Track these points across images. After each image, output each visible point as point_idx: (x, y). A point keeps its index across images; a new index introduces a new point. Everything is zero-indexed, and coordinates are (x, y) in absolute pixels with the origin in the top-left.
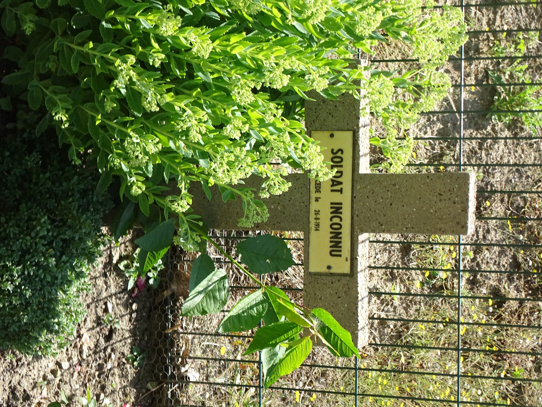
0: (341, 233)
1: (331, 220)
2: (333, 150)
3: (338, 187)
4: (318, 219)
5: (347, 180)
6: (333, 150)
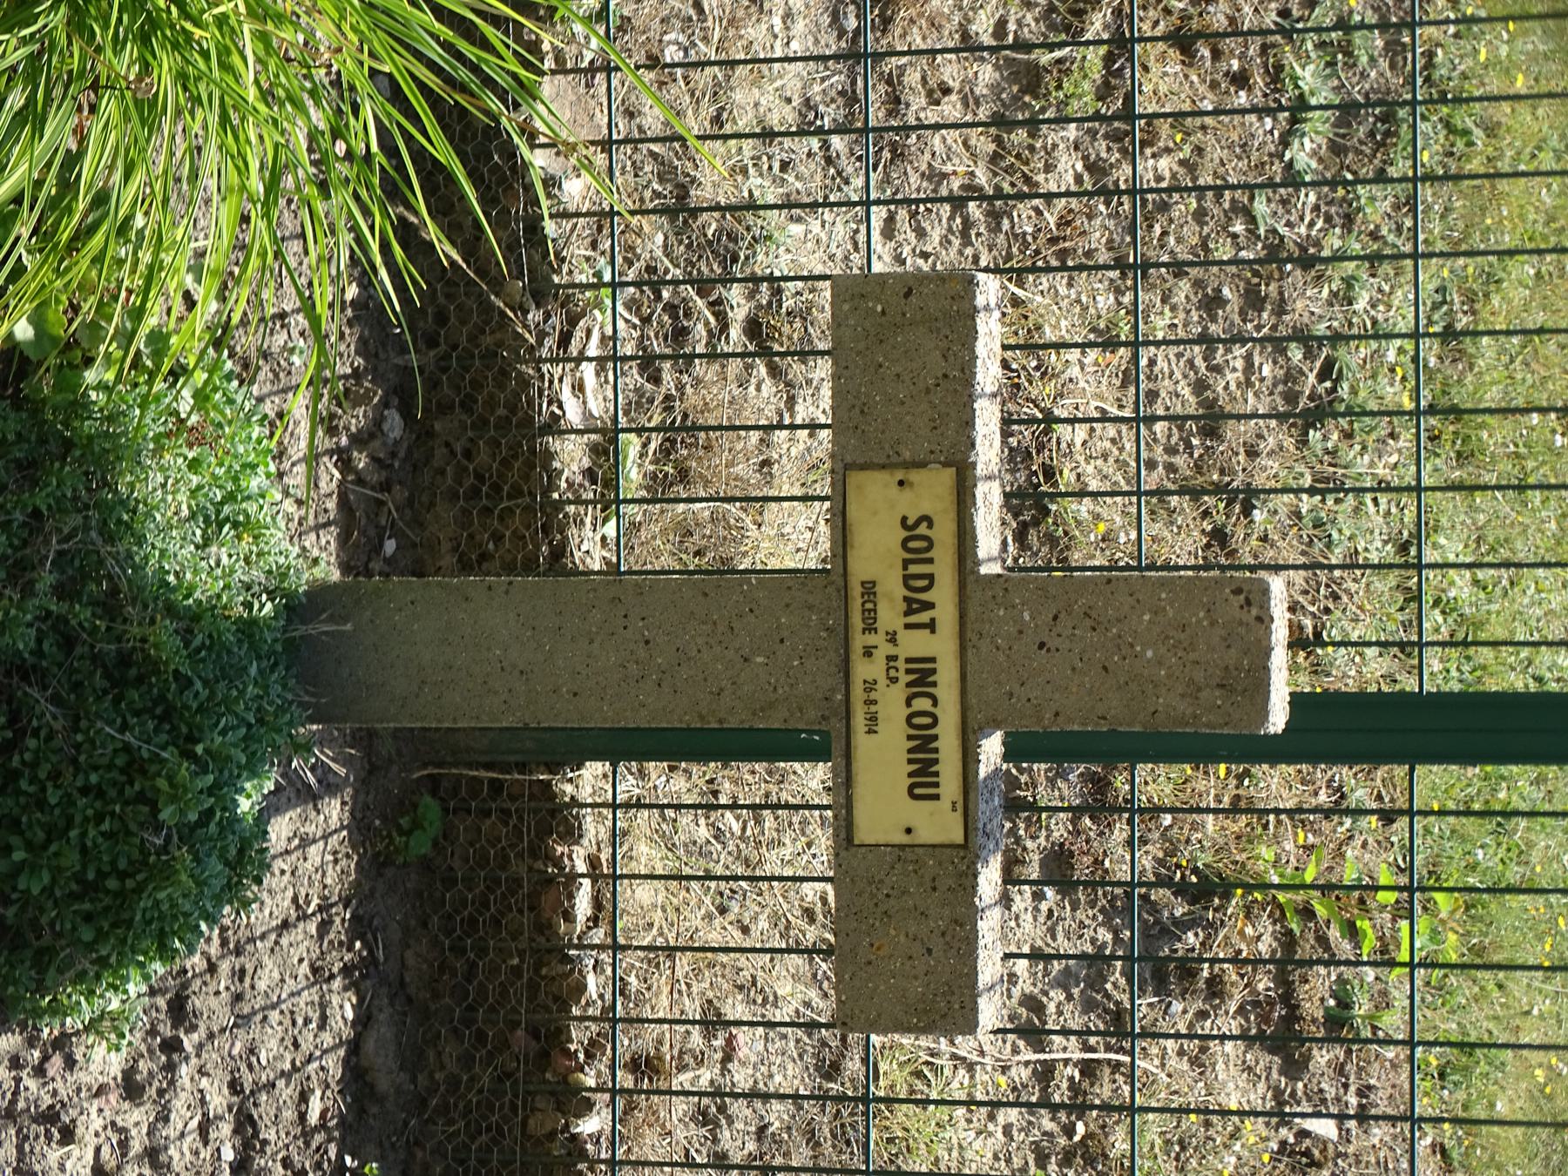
0: (936, 737)
1: (908, 704)
2: (904, 519)
3: (924, 617)
4: (875, 702)
5: (944, 596)
6: (904, 519)
